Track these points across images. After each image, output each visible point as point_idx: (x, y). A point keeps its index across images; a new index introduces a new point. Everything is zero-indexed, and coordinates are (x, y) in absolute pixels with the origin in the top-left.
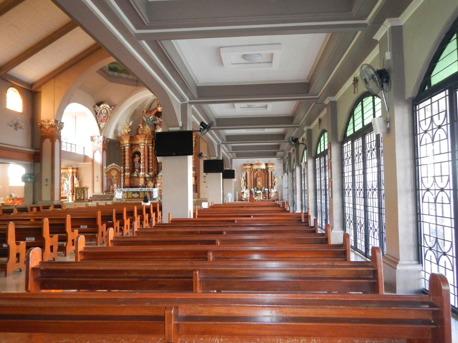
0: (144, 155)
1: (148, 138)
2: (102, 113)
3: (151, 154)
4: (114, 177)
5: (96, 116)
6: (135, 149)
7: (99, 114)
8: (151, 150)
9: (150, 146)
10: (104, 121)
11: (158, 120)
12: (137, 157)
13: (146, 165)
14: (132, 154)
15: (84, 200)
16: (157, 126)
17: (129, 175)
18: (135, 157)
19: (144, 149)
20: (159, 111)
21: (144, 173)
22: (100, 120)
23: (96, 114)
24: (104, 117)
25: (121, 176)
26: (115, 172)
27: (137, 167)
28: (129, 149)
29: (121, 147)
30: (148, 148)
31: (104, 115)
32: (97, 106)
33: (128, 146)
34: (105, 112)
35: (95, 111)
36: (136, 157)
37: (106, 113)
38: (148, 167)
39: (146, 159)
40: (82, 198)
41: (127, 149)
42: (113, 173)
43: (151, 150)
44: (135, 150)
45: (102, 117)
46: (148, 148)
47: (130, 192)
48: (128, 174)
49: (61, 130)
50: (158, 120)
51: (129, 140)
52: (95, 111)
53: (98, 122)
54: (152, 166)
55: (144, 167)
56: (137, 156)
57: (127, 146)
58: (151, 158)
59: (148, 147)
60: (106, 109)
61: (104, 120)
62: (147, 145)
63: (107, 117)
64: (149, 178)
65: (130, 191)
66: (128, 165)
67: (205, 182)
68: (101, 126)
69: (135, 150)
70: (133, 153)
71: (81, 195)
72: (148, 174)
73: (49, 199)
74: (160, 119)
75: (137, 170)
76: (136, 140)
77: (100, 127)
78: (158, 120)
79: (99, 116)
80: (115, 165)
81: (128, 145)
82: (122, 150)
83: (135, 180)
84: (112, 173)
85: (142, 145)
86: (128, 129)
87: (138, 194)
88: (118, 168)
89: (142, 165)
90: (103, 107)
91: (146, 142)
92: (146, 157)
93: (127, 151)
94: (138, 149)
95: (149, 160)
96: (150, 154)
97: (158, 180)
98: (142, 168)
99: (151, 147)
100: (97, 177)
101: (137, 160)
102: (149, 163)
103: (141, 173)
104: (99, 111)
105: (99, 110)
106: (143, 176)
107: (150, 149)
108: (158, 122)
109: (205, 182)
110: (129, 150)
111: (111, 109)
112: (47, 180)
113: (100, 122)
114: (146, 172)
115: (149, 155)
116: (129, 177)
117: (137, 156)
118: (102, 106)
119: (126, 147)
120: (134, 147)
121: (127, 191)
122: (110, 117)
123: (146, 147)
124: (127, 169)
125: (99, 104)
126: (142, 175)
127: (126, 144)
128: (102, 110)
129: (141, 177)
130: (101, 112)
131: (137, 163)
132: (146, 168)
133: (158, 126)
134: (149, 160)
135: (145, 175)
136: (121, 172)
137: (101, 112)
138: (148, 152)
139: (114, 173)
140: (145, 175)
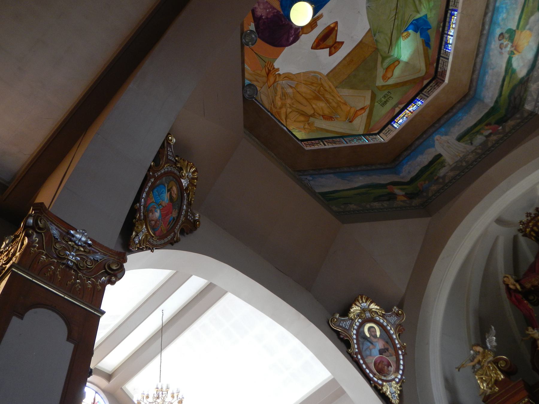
2: (365, 338)
22: (372, 367)
24: (381, 352)
31: (380, 345)
35: (338, 333)
49: (109, 287)
60: (372, 320)
61: (389, 365)
63: (391, 350)
79: (360, 352)
90: (359, 315)
105: (351, 326)
113: (374, 375)
125: (345, 312)
128: (362, 325)
137: (360, 333)
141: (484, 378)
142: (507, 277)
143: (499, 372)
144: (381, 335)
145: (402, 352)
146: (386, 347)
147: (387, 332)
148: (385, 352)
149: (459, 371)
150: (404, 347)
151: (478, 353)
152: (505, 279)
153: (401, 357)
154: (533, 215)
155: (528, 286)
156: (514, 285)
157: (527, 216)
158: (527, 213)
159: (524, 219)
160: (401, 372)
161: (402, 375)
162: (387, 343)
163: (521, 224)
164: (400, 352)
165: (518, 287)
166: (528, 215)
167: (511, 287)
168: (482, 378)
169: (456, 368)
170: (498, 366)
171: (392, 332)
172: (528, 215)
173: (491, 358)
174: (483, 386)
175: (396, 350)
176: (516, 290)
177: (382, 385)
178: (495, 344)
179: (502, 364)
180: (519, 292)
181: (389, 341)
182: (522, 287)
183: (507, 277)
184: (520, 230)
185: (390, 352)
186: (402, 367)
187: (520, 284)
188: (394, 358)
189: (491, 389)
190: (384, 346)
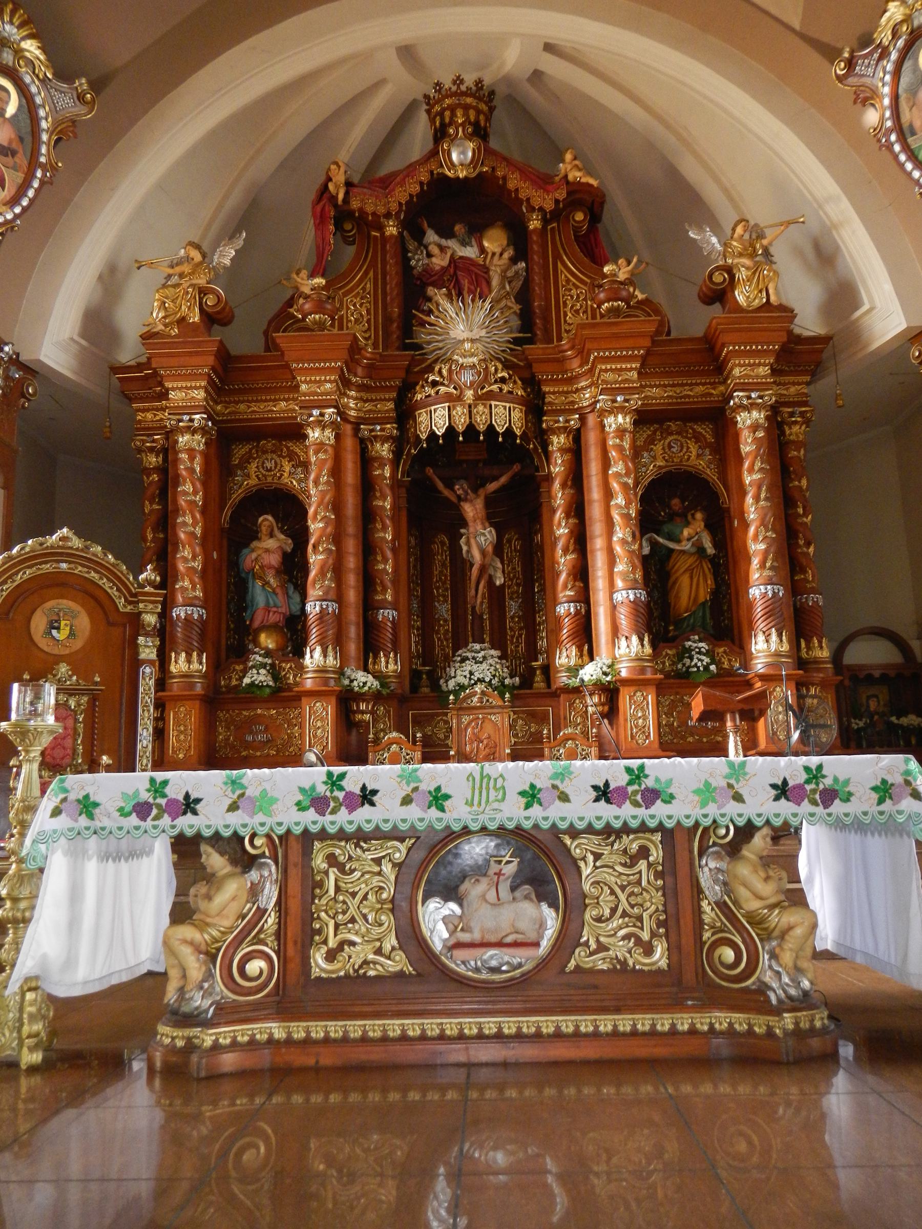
0: (337, 506)
1: (371, 370)
4: (63, 669)
6: (253, 467)
9: (384, 440)
11: (435, 250)
12: (271, 535)
13: (352, 595)
14: (227, 512)
16: (431, 291)
17: (205, 676)
18: (254, 535)
20: (450, 174)
21: (332, 661)
25: (136, 663)
26: (73, 616)
27: (267, 609)
28: (206, 456)
29: (139, 451)
30: (366, 461)
33: (203, 430)
38: (369, 606)
39: (351, 546)
41: (191, 452)
44: (253, 481)
46: (366, 461)
47: (378, 835)
48: (195, 666)
50: (442, 249)
51: (211, 381)
54: (395, 606)
55: (332, 607)
56: (266, 520)
59: (363, 446)
62: (356, 430)
63: (22, 160)
64: (376, 697)
65: (364, 816)
66: (199, 593)
70: (237, 495)
72: (366, 670)
74: (452, 243)
75: (267, 641)
76: (268, 390)
78: (442, 249)
80: (76, 542)
82: (147, 471)
83: (256, 720)
84: (39, 623)
85: (321, 424)
87: (544, 895)
88: (105, 583)
89: (314, 592)
91: (351, 404)
92: (351, 528)
93: (192, 470)
97: (465, 719)
98: (323, 613)
99: (384, 450)
101: (274, 559)
102: (369, 581)
103: (314, 658)
106: (326, 681)
108: (439, 261)
110: (206, 470)
114: (353, 648)
115: (368, 515)
116: (199, 689)
117: (266, 520)
119: (183, 440)
121: (310, 819)
123: (349, 443)
124: (188, 620)
126: (321, 670)
127: (191, 410)
129: (311, 694)
132: (353, 616)
133: (439, 296)
134: (368, 549)
135: (340, 672)
136: (135, 619)
138: (367, 487)
140: (340, 672)
141: (167, 305)
142: (339, 167)
143: (197, 310)
144: (15, 116)
145: (44, 175)
146: (14, 146)
147: (34, 120)
148: (6, 155)
149: (139, 268)
150: (54, 169)
151: (188, 259)
152: (333, 167)
153: (36, 184)
154: (463, 88)
155: (355, 204)
156: (337, 187)
157: (454, 82)
158: (458, 77)
159: (448, 84)
160: (18, 210)
161: (16, 216)
162: (21, 139)
163: (435, 88)
164: (39, 174)
165: (341, 196)
166: (458, 81)
167: (331, 186)
168: (165, 303)
169: (136, 261)
170: (201, 299)
171: (44, 125)
172: (458, 81)
173: (202, 281)
174: (157, 314)
175: (33, 163)
176: (334, 198)
178: (227, 262)
179: (210, 301)
180: (336, 206)
181: (28, 139)
182: (346, 200)
183: (339, 167)
184: (426, 97)
185: (17, 159)
186: (25, 202)
187: (347, 193)
188: (20, 177)
189: (166, 325)
190: (10, 142)
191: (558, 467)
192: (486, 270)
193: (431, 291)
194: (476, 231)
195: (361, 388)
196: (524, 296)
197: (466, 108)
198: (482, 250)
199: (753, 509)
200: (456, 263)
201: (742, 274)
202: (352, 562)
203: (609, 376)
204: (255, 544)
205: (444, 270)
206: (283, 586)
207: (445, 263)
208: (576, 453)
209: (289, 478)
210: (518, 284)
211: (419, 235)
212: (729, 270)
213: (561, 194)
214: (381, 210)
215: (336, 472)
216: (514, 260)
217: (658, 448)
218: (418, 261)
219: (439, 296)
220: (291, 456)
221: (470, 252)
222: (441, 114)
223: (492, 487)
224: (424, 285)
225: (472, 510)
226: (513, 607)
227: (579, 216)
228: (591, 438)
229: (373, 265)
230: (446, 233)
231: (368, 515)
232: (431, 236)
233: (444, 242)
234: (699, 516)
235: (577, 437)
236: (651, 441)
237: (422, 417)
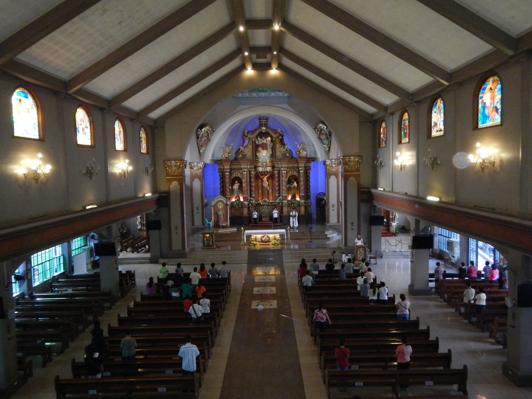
3: (253, 180)
5: (197, 141)
6: (234, 174)
7: (201, 138)
8: (253, 176)
10: (204, 145)
12: (237, 184)
15: (213, 246)
18: (235, 183)
19: (247, 174)
22: (200, 144)
23: (198, 138)
24: (205, 141)
30: (250, 174)
31: (205, 139)
32: (199, 130)
34: (206, 135)
36: (236, 183)
37: (206, 137)
39: (249, 186)
40: (211, 244)
41: (227, 175)
42: (219, 206)
43: (253, 176)
44: (234, 176)
45: (203, 141)
46: (250, 174)
52: (197, 135)
53: (198, 147)
56: (236, 182)
57: (228, 172)
58: (253, 184)
59: (250, 172)
63: (207, 141)
67: (352, 229)
68: (201, 151)
69: (234, 175)
71: (209, 241)
73: (180, 248)
74: (262, 140)
77: (200, 152)
78: (261, 141)
81: (229, 170)
84: (218, 205)
86: (229, 153)
90: (204, 130)
92: (249, 184)
94: (238, 174)
95: (251, 186)
96: (252, 180)
100: (197, 208)
101: (237, 187)
104: (201, 135)
107: (252, 174)
108: (260, 143)
109: (352, 229)
111: (211, 132)
112: (176, 227)
115: (250, 181)
117: (236, 182)
118: (203, 129)
120: (233, 173)
122: (210, 140)
123: (248, 172)
125: (201, 127)
127: (227, 169)
130: (202, 135)
131: (238, 190)
133: (260, 149)
134: (251, 186)
138: (250, 177)
139: (221, 206)
176: (245, 135)
177: (200, 150)
191: (277, 175)
192: (267, 144)
193: (259, 148)
194: (266, 137)
195: (250, 164)
196: (272, 149)
197: (264, 122)
198: (266, 141)
199: (302, 183)
200: (263, 143)
201: (301, 152)
202: (249, 188)
203: (283, 166)
204: (235, 185)
205: (261, 144)
206: (239, 190)
207: (261, 143)
208: (279, 173)
209: (239, 175)
210: (271, 146)
211: (257, 138)
212: (299, 151)
213: (278, 135)
214: (252, 137)
215: (247, 177)
216: (271, 143)
217: (290, 172)
218: (257, 143)
219: (260, 149)
220: (240, 172)
221: (265, 142)
222: (261, 122)
223: (267, 176)
224: (258, 147)
225: (265, 179)
226: (270, 191)
227: (280, 137)
228: (281, 171)
229: (251, 144)
230: (261, 138)
231: (250, 181)
232: (259, 139)
233: (261, 140)
234: (295, 182)
235: (279, 171)
236: (289, 171)
237: (258, 168)
